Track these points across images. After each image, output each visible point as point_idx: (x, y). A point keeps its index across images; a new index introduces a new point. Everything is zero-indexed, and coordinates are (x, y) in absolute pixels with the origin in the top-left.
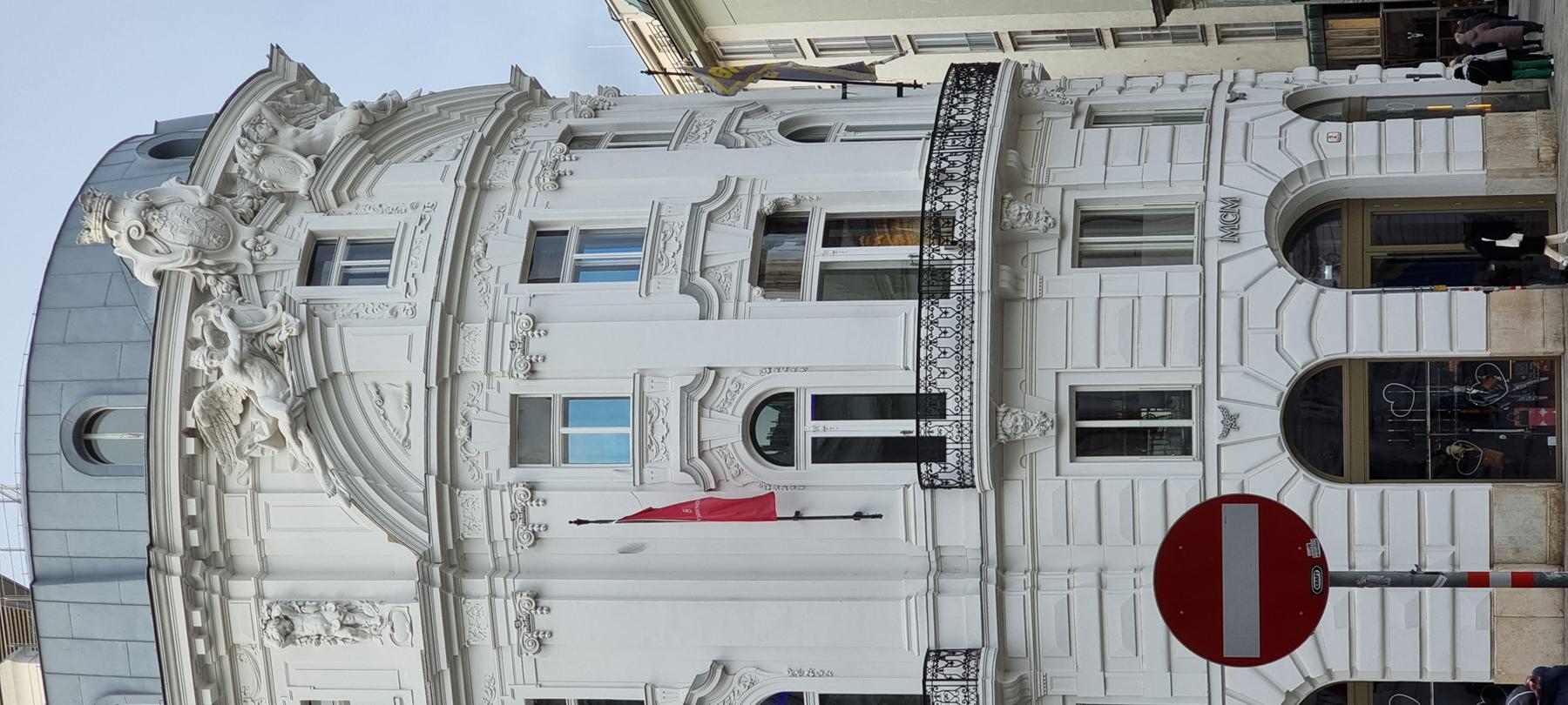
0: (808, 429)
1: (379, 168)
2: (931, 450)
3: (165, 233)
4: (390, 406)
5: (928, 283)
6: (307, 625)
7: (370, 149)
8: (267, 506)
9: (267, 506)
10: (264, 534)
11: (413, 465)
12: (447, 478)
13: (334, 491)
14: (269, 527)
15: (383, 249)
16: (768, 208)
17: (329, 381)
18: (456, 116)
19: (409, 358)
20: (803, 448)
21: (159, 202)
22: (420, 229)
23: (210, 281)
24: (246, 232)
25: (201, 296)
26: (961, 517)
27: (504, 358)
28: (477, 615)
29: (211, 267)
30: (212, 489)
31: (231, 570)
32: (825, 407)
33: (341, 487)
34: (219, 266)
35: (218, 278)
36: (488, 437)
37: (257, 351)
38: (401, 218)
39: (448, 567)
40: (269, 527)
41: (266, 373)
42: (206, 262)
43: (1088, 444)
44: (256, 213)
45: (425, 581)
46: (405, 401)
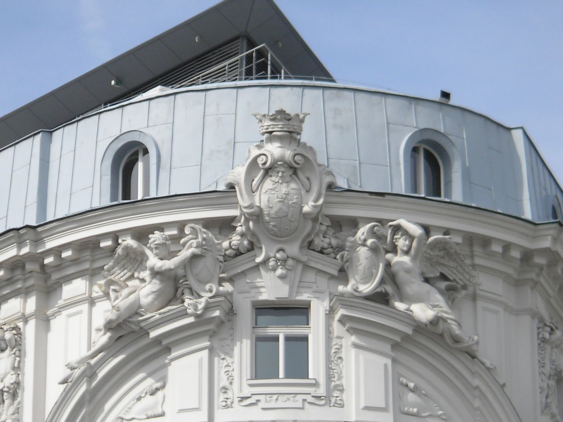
1: (387, 348)
3: (268, 184)
4: (148, 400)
7: (406, 337)
8: (80, 312)
9: (80, 312)
10: (65, 313)
13: (72, 369)
14: (69, 316)
15: (298, 368)
17: (164, 347)
18: (477, 403)
19: (181, 411)
21: (300, 173)
22: (310, 399)
23: (239, 229)
24: (294, 249)
25: (225, 226)
29: (248, 228)
30: (87, 266)
33: (77, 372)
34: (254, 235)
35: (242, 235)
37: (174, 286)
38: (322, 380)
40: (69, 316)
41: (159, 294)
42: (251, 224)
44: (321, 252)
46: (150, 414)
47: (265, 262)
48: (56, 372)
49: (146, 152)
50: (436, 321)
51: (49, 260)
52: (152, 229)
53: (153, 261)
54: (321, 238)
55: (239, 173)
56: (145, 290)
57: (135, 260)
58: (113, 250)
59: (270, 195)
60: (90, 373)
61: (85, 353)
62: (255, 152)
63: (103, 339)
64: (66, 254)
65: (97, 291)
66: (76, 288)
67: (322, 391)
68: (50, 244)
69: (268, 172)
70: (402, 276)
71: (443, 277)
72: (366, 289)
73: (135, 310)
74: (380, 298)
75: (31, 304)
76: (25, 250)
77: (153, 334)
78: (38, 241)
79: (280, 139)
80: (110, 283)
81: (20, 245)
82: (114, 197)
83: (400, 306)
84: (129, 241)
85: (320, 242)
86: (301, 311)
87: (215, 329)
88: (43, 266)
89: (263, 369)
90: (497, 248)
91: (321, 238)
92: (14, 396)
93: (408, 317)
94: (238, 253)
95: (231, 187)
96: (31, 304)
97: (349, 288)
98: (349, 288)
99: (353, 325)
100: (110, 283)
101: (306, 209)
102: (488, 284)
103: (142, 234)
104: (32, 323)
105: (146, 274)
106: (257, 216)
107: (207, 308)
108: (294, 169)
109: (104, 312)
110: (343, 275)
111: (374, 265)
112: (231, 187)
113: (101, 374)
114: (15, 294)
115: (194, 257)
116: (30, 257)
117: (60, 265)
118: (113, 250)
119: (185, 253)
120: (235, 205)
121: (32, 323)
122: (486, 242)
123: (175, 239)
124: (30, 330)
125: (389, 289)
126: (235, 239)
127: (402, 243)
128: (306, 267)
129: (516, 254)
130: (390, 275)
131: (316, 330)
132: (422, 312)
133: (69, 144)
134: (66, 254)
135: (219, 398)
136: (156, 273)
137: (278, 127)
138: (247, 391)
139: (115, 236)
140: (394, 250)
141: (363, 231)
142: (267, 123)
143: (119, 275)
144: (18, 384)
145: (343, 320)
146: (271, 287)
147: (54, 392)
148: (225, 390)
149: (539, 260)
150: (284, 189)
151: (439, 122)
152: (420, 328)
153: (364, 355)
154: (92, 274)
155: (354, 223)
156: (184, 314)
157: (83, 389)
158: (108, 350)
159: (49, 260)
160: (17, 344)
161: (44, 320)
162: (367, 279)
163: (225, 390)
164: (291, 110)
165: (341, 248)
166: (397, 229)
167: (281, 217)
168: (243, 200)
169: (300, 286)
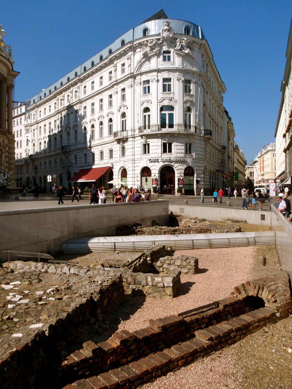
0: (147, 114)
2: (145, 129)
3: (165, 32)
4: (148, 65)
5: (163, 125)
6: (129, 60)
11: (143, 69)
12: (141, 74)
15: (169, 60)
16: (173, 106)
20: (145, 114)
24: (169, 43)
25: (159, 39)
26: (137, 132)
27: (152, 78)
28: (130, 80)
31: (135, 51)
32: (149, 116)
36: (145, 78)
37: (152, 49)
39: (134, 77)
41: (150, 50)
43: (145, 145)
45: (131, 74)
47: (165, 45)
48: (136, 62)
49: (148, 30)
50: (188, 53)
51: (134, 46)
52: (149, 40)
53: (149, 45)
54: (172, 42)
55: (161, 31)
56: (148, 49)
57: (146, 45)
58: (143, 44)
59: (165, 34)
60: (141, 62)
61: (140, 59)
62: (163, 28)
63: (142, 56)
64: (137, 45)
65: (141, 50)
66: (138, 50)
67: (172, 63)
68: (134, 44)
69: (165, 31)
70: (183, 46)
71: (189, 47)
72: (179, 48)
73: (146, 52)
74: (181, 50)
75: (132, 53)
76: (131, 45)
77: (149, 55)
78: (133, 43)
79: (167, 26)
80: (143, 49)
81: (131, 44)
82: (143, 36)
83: (183, 51)
84: (146, 42)
85: (172, 42)
86: (169, 52)
87: (158, 55)
88: (134, 47)
89: (164, 60)
90: (197, 43)
91: (172, 42)
92: (130, 66)
93: (184, 53)
94: (161, 43)
95: (160, 33)
96: (132, 53)
97: (176, 48)
98: (176, 48)
99: (177, 54)
100: (143, 49)
101: (170, 36)
102: (195, 48)
103: (147, 41)
104: (132, 55)
105: (148, 47)
106: (163, 38)
107: (157, 51)
108: (169, 30)
109: (142, 53)
110: (176, 46)
111: (180, 45)
112: (160, 33)
113: (142, 62)
114: (130, 51)
115: (155, 44)
116: (132, 46)
117: (136, 46)
118: (143, 44)
119: (154, 43)
120: (160, 36)
121: (132, 55)
122: (195, 42)
123: (152, 42)
124: (132, 57)
125: (182, 48)
126: (160, 41)
127: (184, 41)
128: (170, 45)
129: (199, 44)
130: (182, 46)
131: (171, 55)
132: (186, 51)
133: (137, 29)
134: (137, 45)
135: (158, 64)
136: (150, 47)
137: (167, 24)
138: (162, 63)
139: (143, 42)
140: (183, 42)
141: (178, 40)
142: (165, 23)
143: (145, 47)
144: (131, 64)
145: (176, 53)
146: (165, 48)
147: (136, 64)
148: (159, 63)
149: (203, 45)
150: (167, 33)
151: (189, 25)
152: (186, 54)
153: (178, 58)
154: (140, 48)
155: (177, 39)
156: (153, 52)
157: (140, 64)
158: (143, 58)
159: (134, 46)
160: (131, 58)
161: (134, 55)
162: (179, 47)
163: (159, 63)
164: (169, 21)
165: (175, 42)
166: (183, 39)
167: (167, 38)
168: (161, 35)
169: (170, 48)
